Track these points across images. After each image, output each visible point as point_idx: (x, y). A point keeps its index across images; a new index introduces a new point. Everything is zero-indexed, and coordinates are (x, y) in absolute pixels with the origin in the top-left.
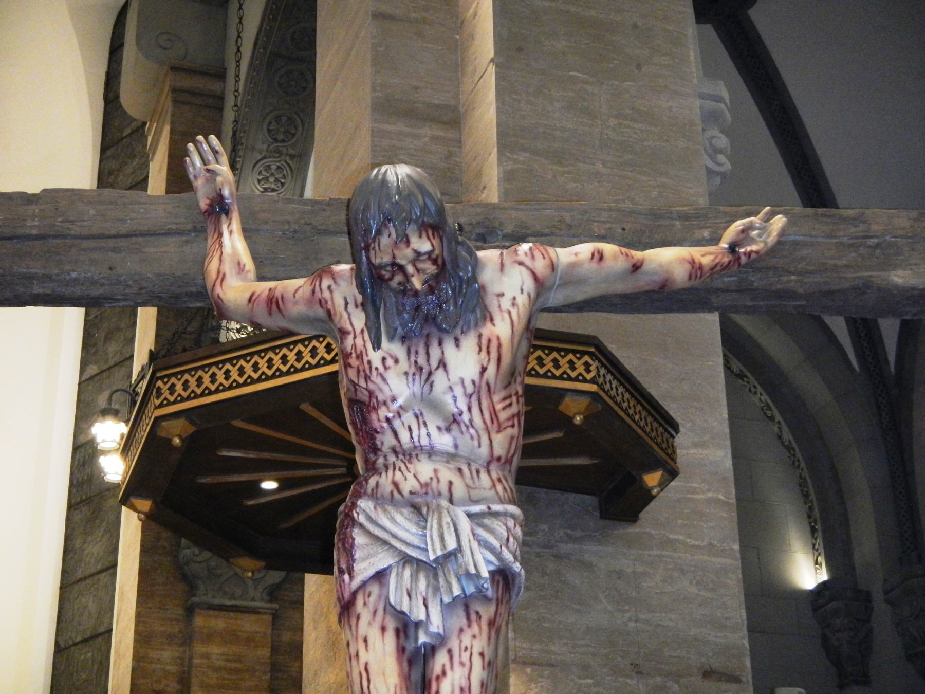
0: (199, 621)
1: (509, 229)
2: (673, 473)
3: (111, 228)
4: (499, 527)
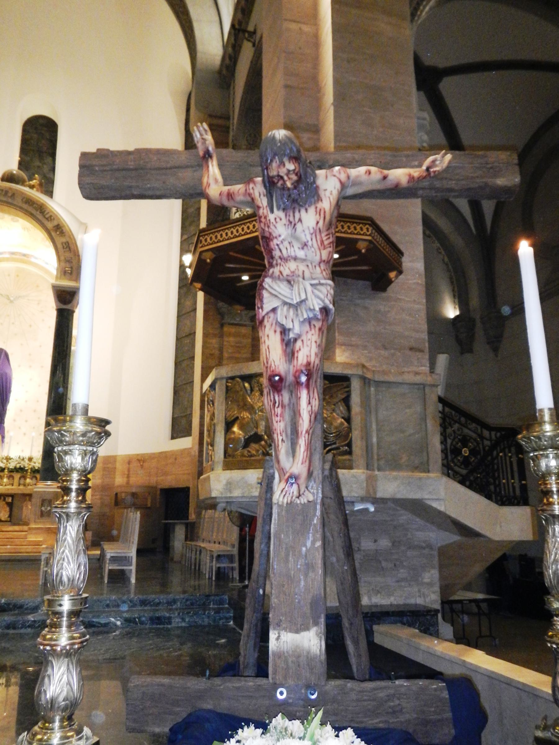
0: (226, 329)
1: (331, 162)
3: (164, 165)
4: (324, 289)
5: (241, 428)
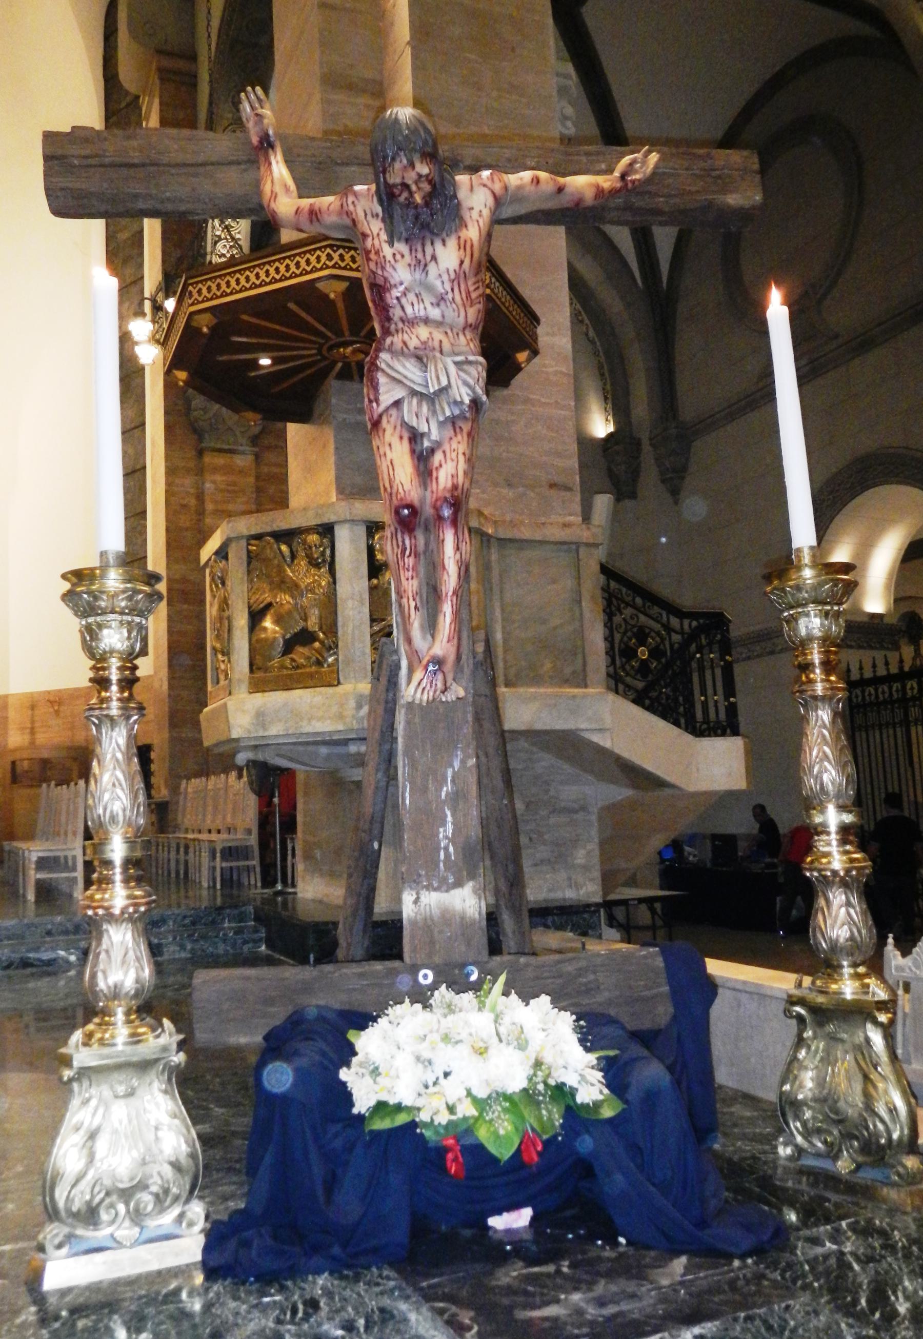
0: (208, 459)
1: (468, 162)
2: (535, 352)
3: (190, 158)
4: (473, 370)
5: (278, 621)
